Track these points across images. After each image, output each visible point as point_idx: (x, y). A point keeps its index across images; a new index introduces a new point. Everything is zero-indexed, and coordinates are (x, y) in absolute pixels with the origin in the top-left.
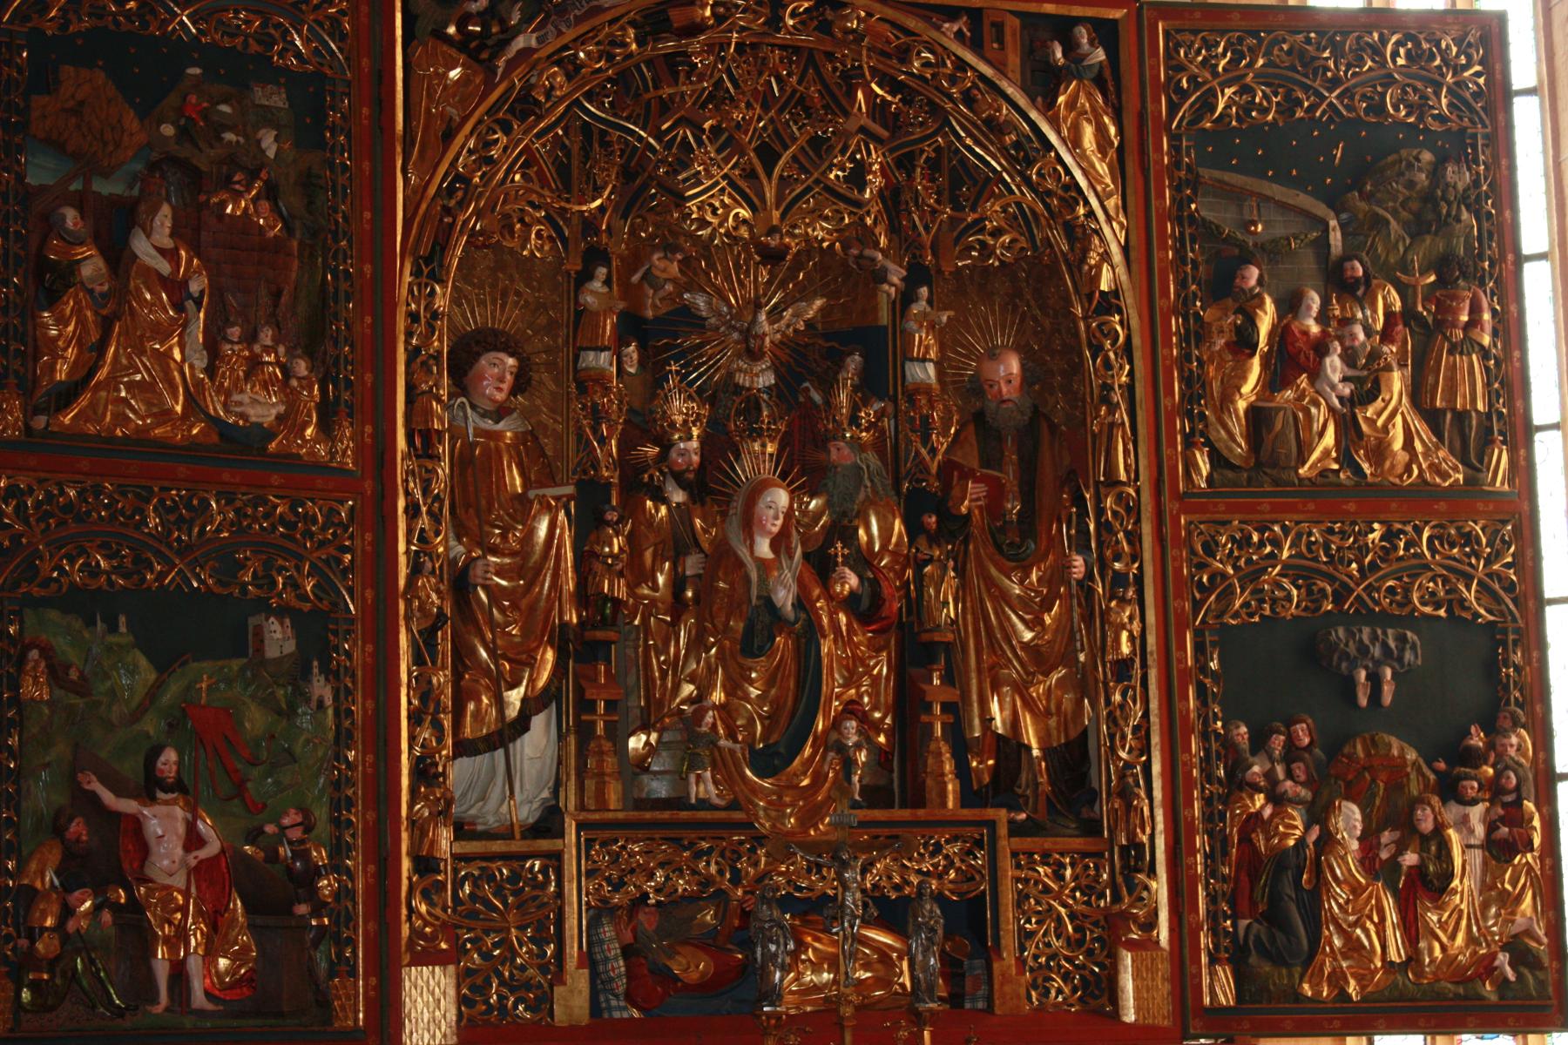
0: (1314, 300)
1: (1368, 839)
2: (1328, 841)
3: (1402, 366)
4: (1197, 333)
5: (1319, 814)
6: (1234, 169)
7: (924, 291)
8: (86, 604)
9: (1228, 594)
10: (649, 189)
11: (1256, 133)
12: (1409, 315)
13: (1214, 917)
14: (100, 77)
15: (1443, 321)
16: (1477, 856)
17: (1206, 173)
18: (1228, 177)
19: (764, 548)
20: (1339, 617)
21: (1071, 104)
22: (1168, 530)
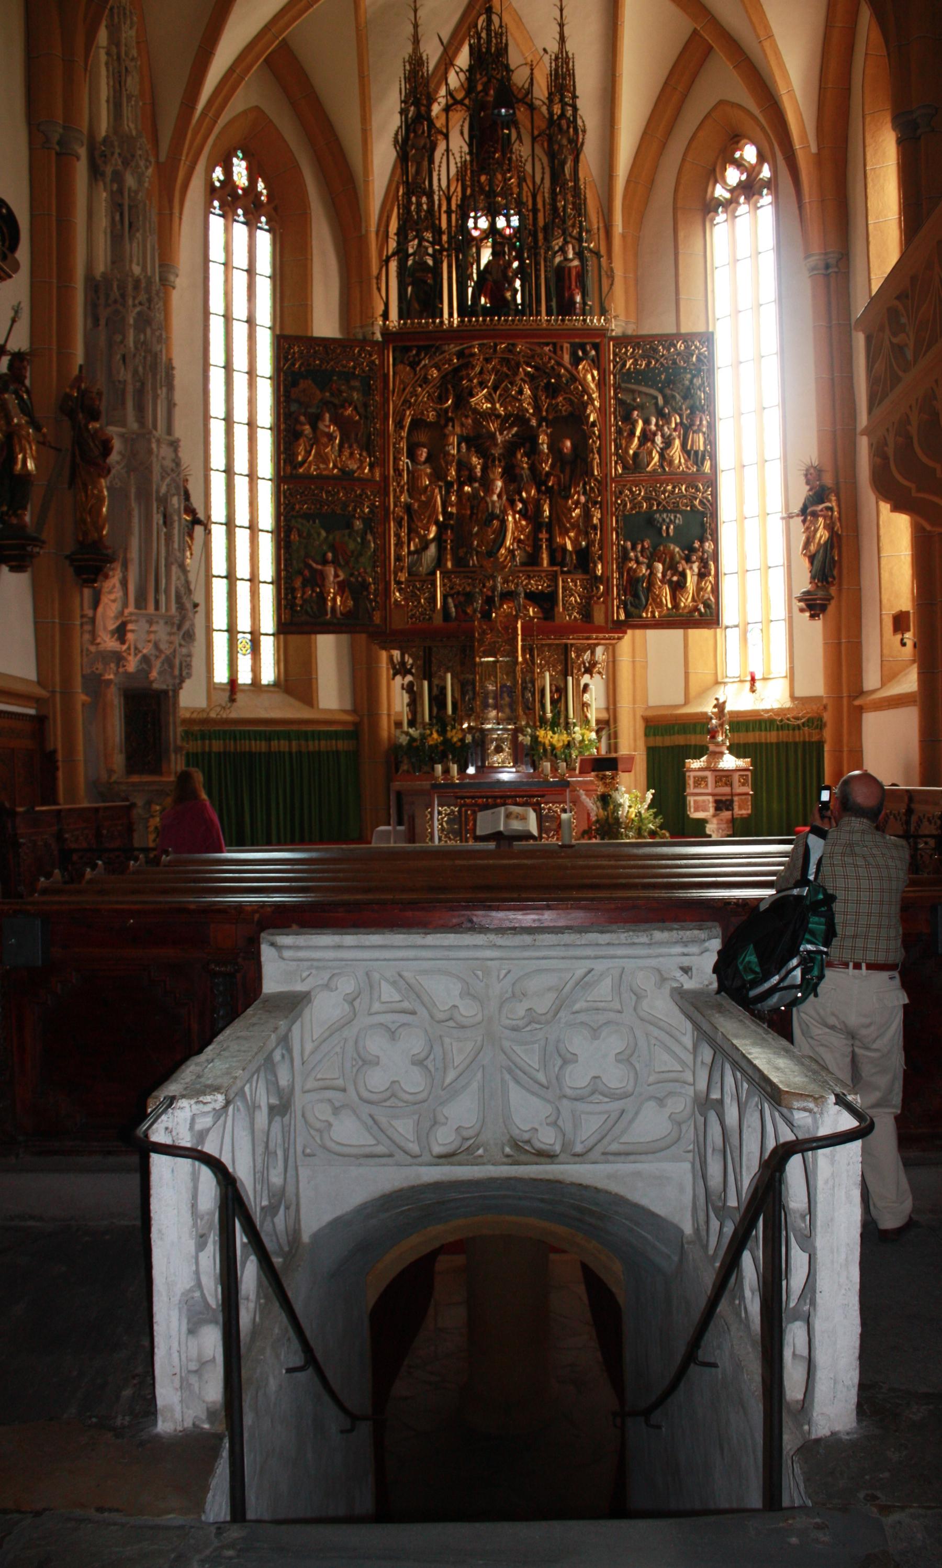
0: (654, 420)
1: (664, 575)
2: (652, 574)
3: (679, 438)
4: (619, 431)
5: (650, 566)
6: (634, 384)
7: (544, 424)
8: (307, 516)
9: (625, 505)
11: (638, 372)
12: (681, 423)
13: (618, 594)
14: (310, 382)
15: (692, 424)
16: (696, 578)
17: (623, 385)
18: (630, 386)
19: (495, 498)
20: (656, 511)
21: (583, 368)
22: (609, 488)
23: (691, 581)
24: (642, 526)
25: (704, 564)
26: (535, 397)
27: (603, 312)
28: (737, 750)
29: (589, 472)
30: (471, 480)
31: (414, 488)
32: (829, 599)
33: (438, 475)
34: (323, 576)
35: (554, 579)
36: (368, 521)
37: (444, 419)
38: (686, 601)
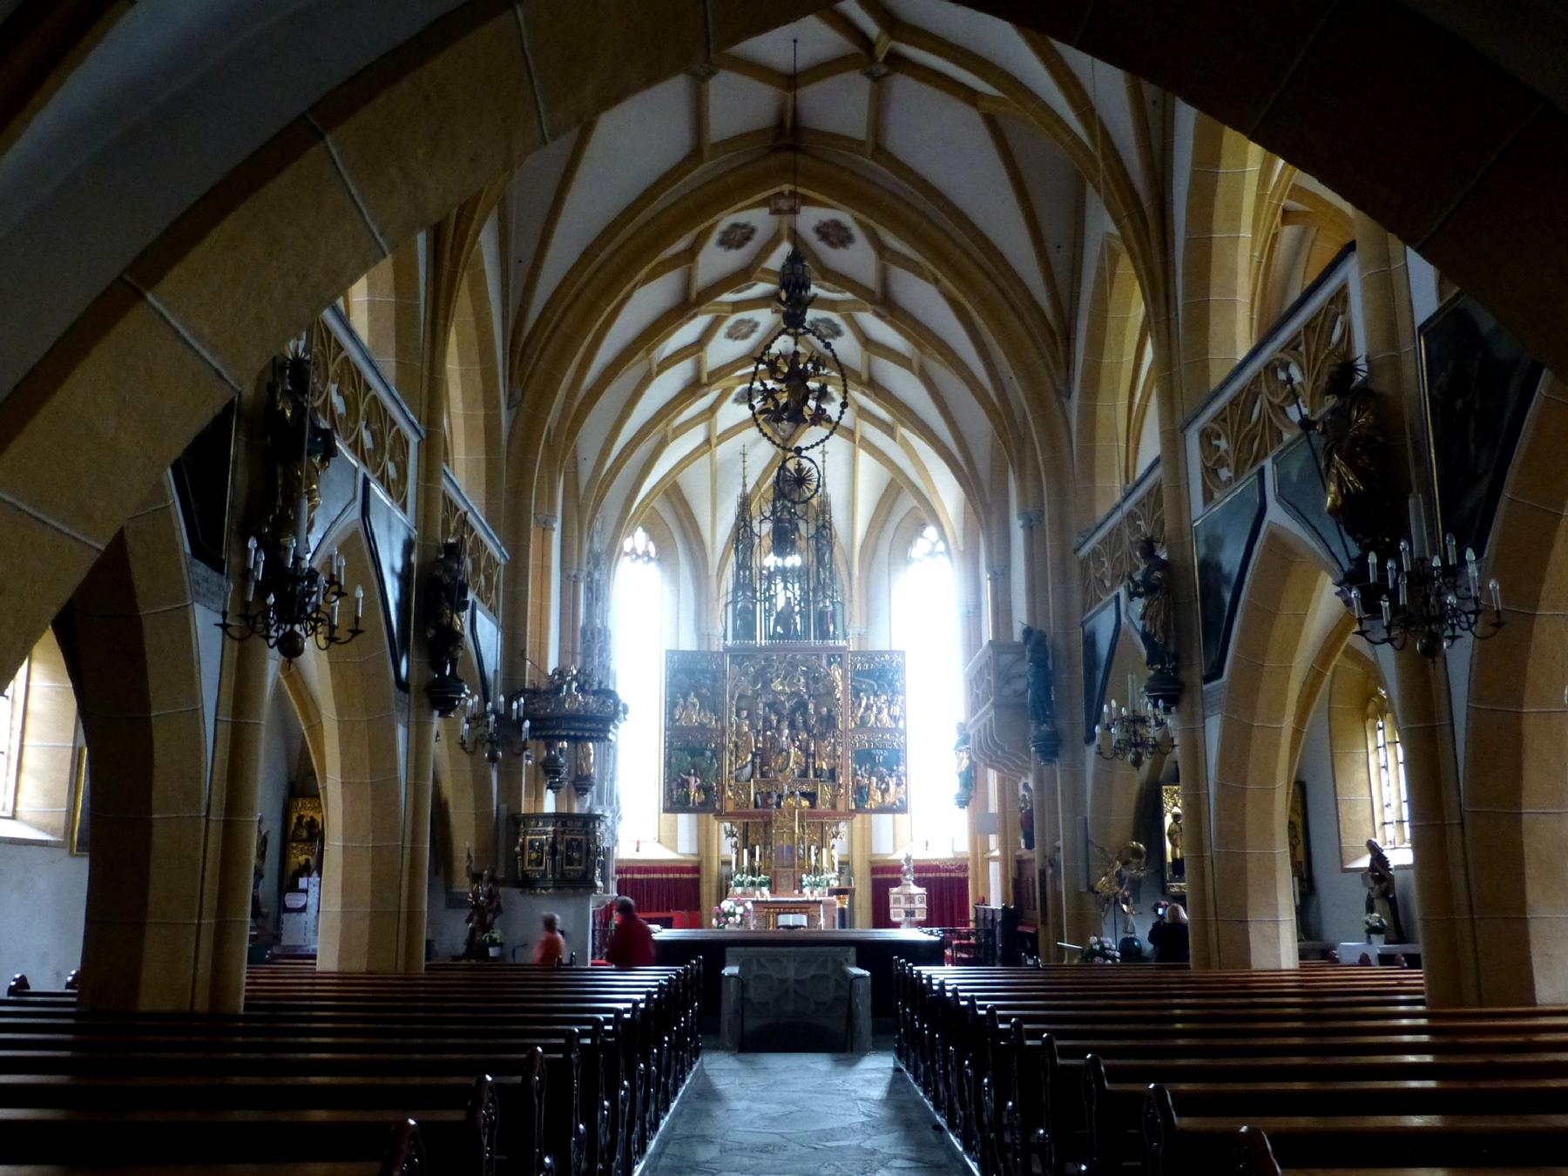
10: (767, 684)
23: (892, 788)
24: (865, 757)
25: (899, 778)
26: (807, 685)
27: (845, 636)
28: (918, 882)
29: (835, 726)
30: (770, 728)
31: (739, 733)
32: (970, 798)
33: (752, 726)
34: (688, 782)
35: (815, 784)
36: (714, 753)
37: (757, 694)
38: (889, 799)
